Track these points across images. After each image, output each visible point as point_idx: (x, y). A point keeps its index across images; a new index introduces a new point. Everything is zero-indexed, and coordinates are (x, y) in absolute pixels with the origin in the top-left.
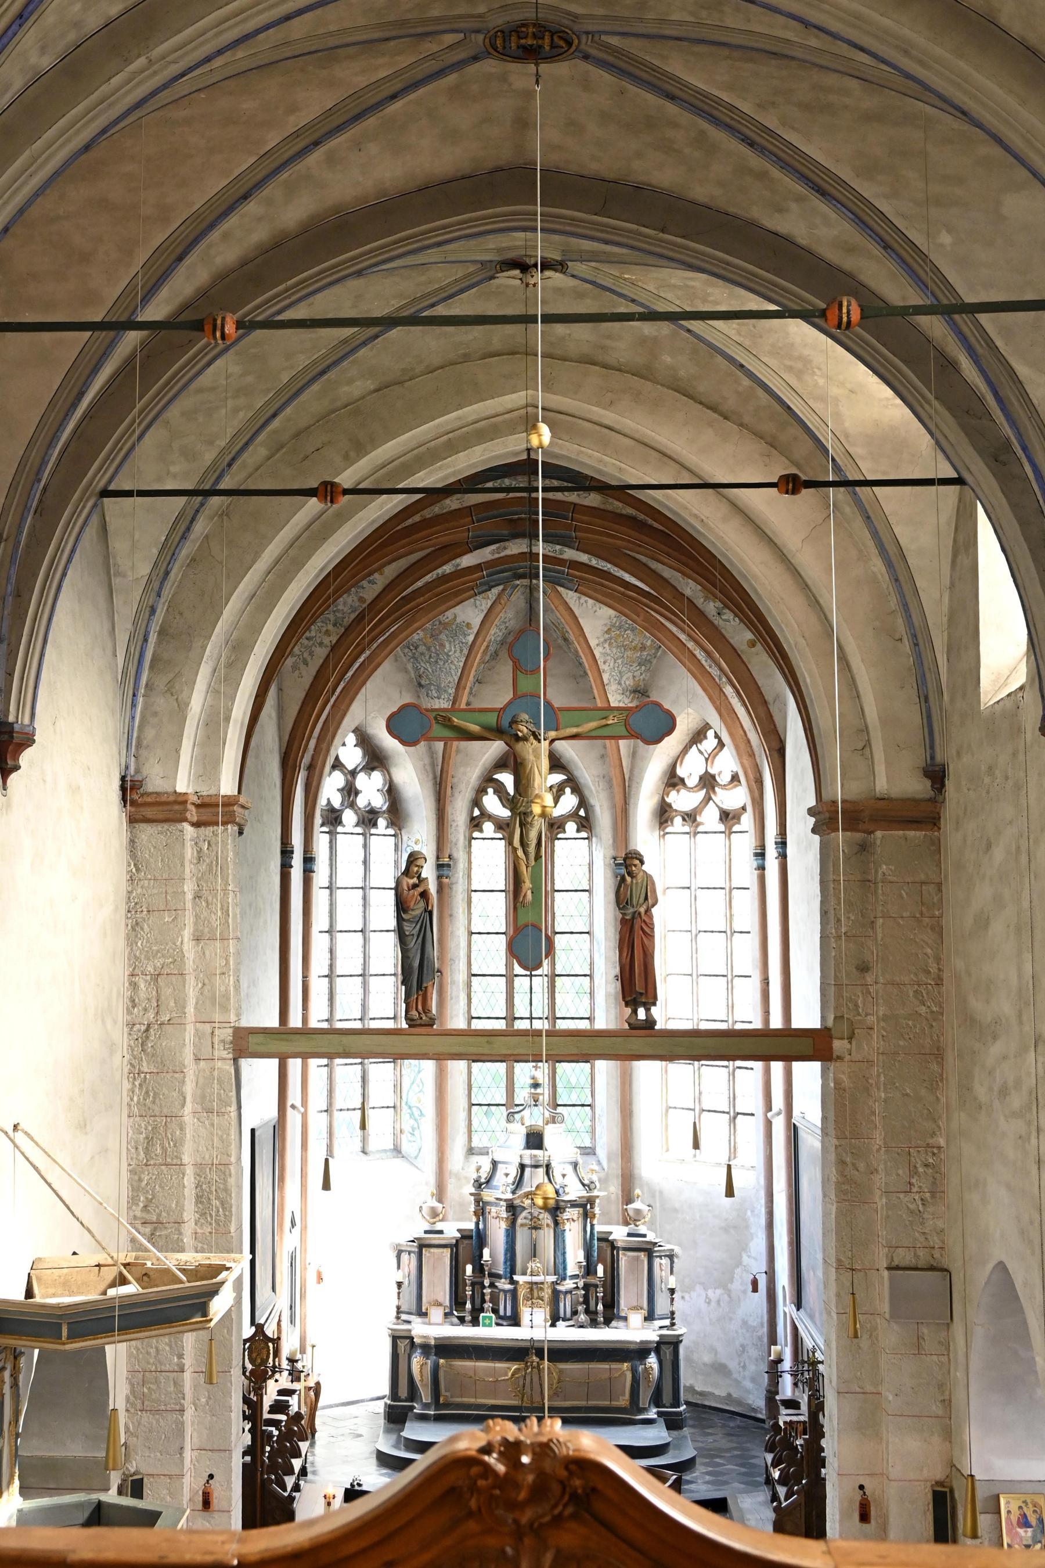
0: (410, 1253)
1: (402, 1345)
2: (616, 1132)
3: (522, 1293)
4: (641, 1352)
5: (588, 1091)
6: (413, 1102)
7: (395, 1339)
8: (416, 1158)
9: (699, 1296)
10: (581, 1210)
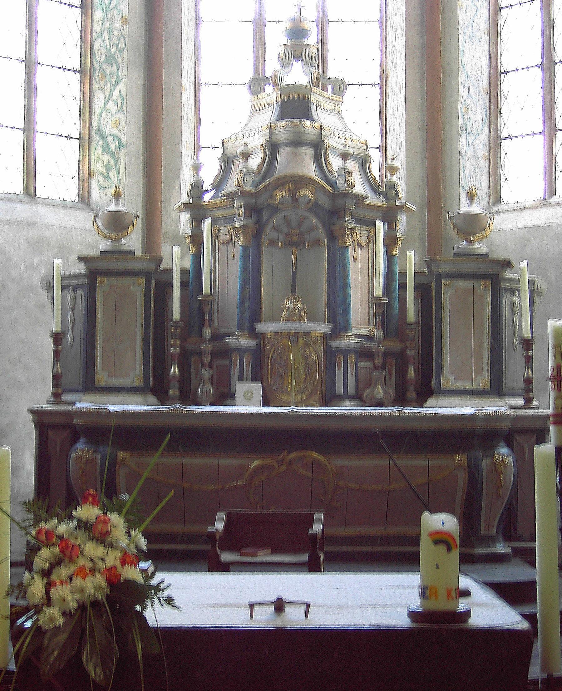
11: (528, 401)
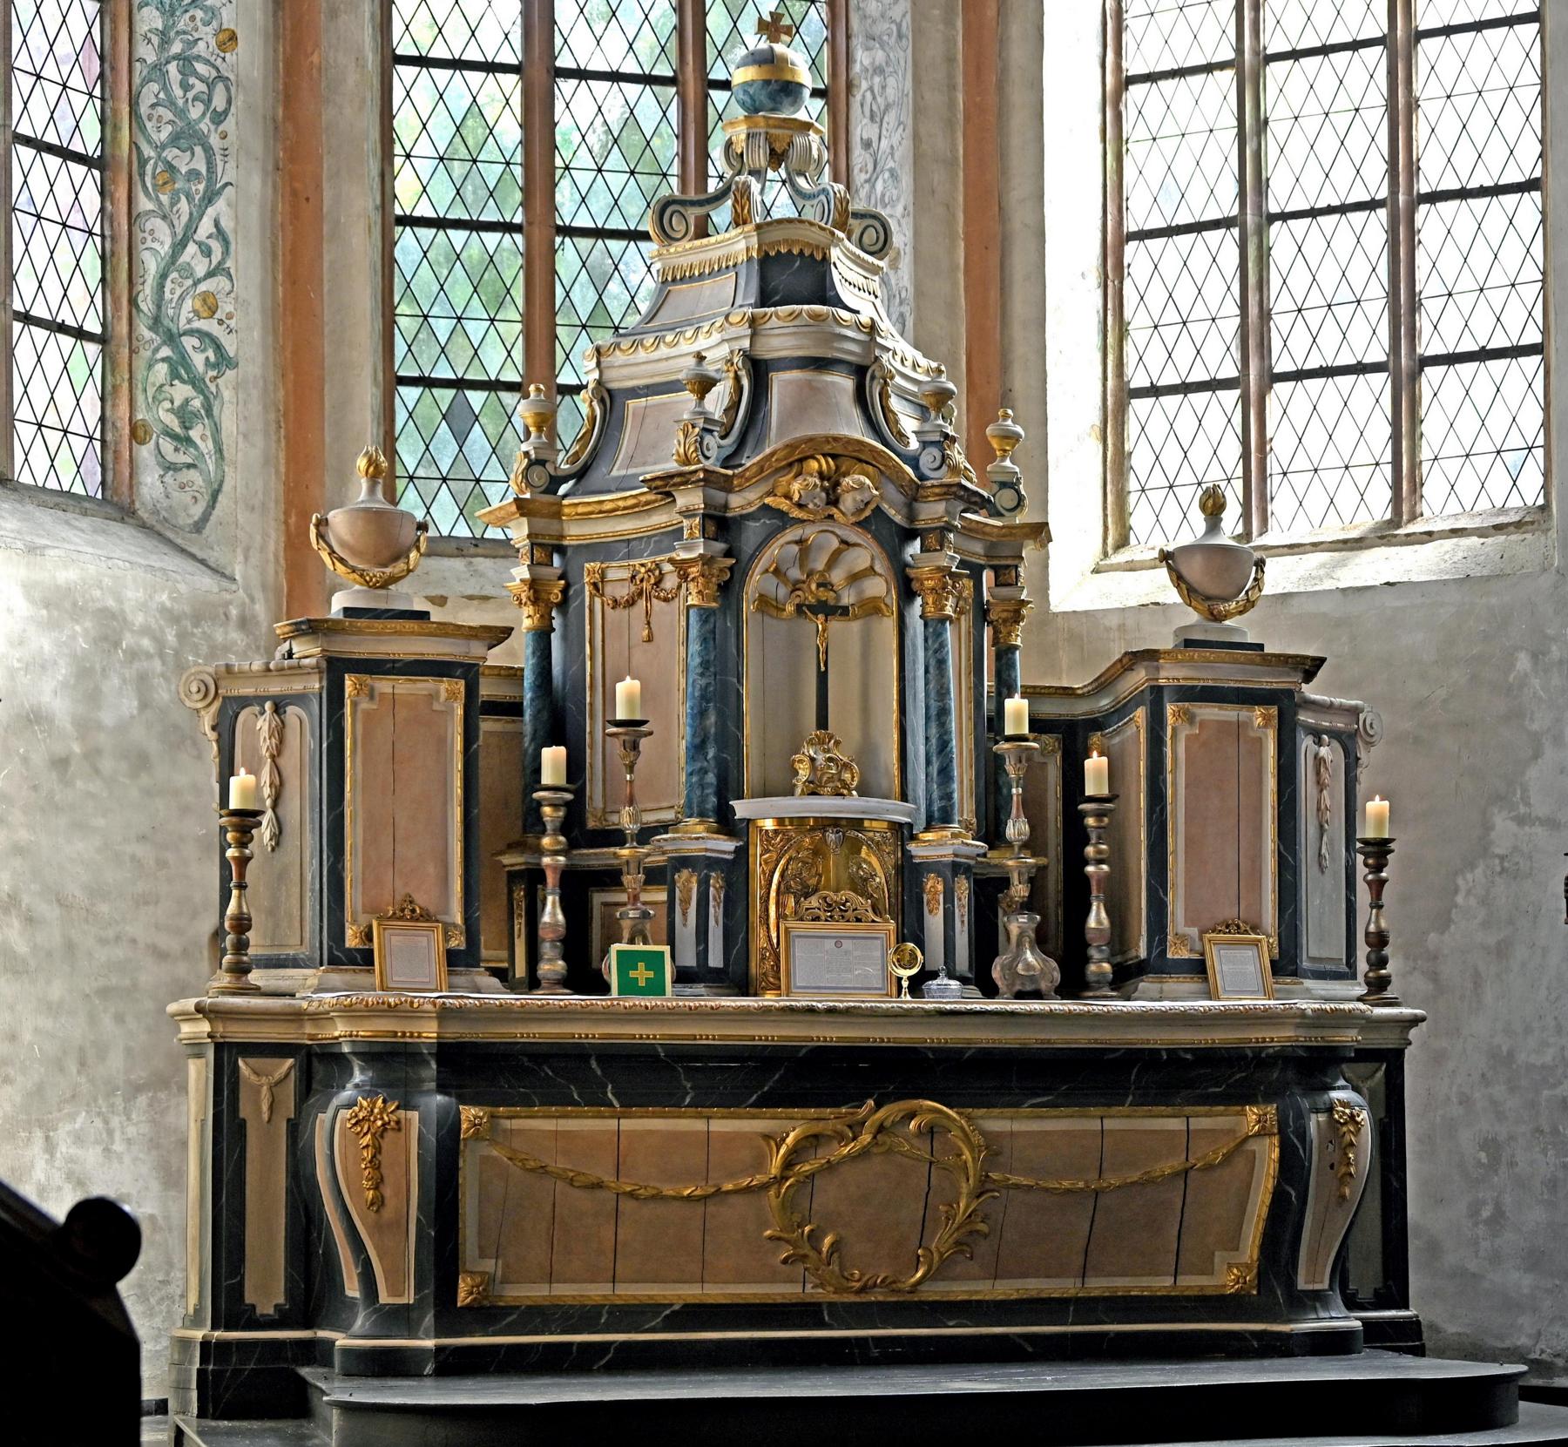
0: (278, 709)
1: (264, 1082)
3: (767, 874)
4: (1313, 1065)
6: (185, 314)
7: (226, 1055)
8: (199, 527)
11: (1378, 985)
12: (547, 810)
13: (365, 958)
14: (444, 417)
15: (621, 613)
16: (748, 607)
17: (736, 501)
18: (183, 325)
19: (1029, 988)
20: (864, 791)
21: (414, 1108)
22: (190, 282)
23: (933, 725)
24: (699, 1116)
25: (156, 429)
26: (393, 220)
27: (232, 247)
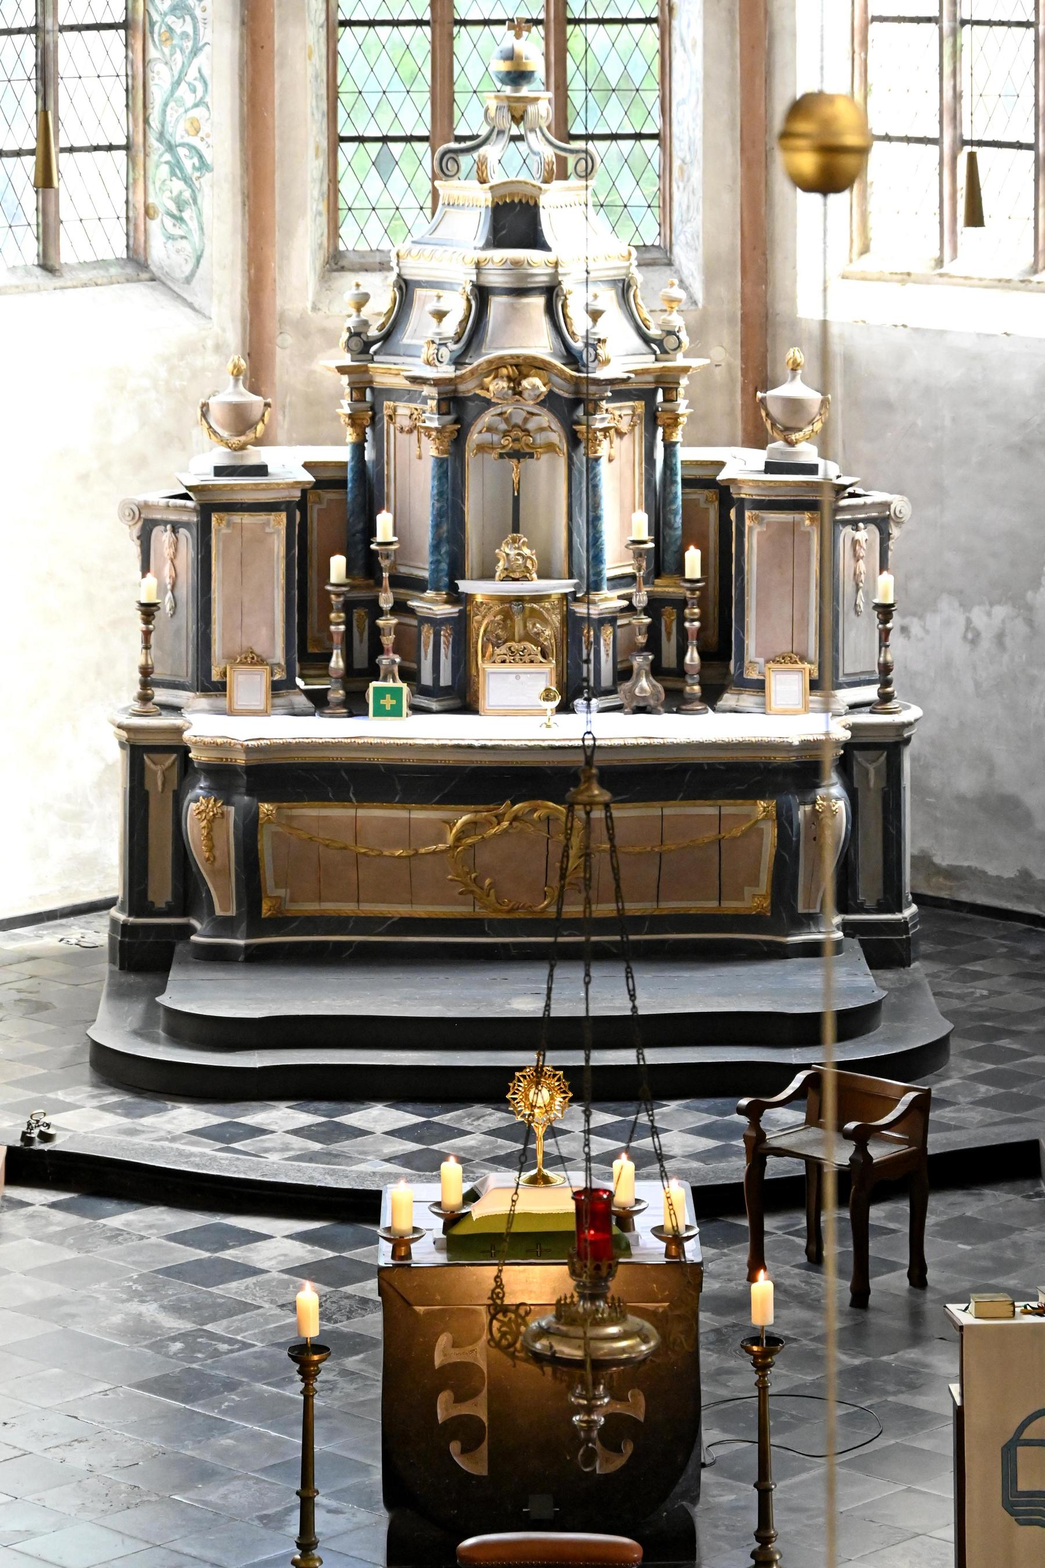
0: (175, 527)
2: (730, 203)
5: (652, 98)
6: (178, 133)
8: (188, 280)
9: (947, 623)
10: (640, 406)
12: (333, 597)
13: (220, 688)
14: (373, 164)
15: (405, 436)
16: (469, 455)
17: (462, 388)
18: (179, 140)
19: (642, 704)
20: (544, 574)
21: (233, 805)
22: (182, 110)
23: (591, 527)
24: (405, 808)
25: (161, 210)
26: (337, 24)
27: (210, 87)
